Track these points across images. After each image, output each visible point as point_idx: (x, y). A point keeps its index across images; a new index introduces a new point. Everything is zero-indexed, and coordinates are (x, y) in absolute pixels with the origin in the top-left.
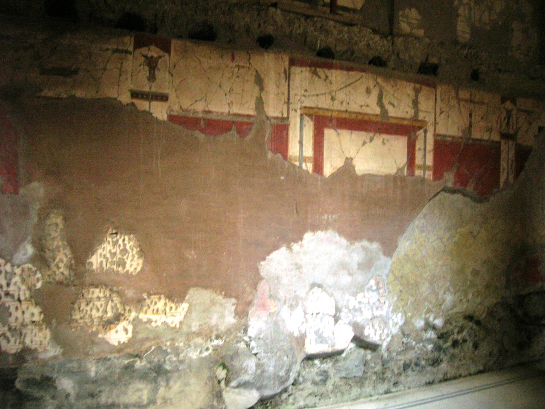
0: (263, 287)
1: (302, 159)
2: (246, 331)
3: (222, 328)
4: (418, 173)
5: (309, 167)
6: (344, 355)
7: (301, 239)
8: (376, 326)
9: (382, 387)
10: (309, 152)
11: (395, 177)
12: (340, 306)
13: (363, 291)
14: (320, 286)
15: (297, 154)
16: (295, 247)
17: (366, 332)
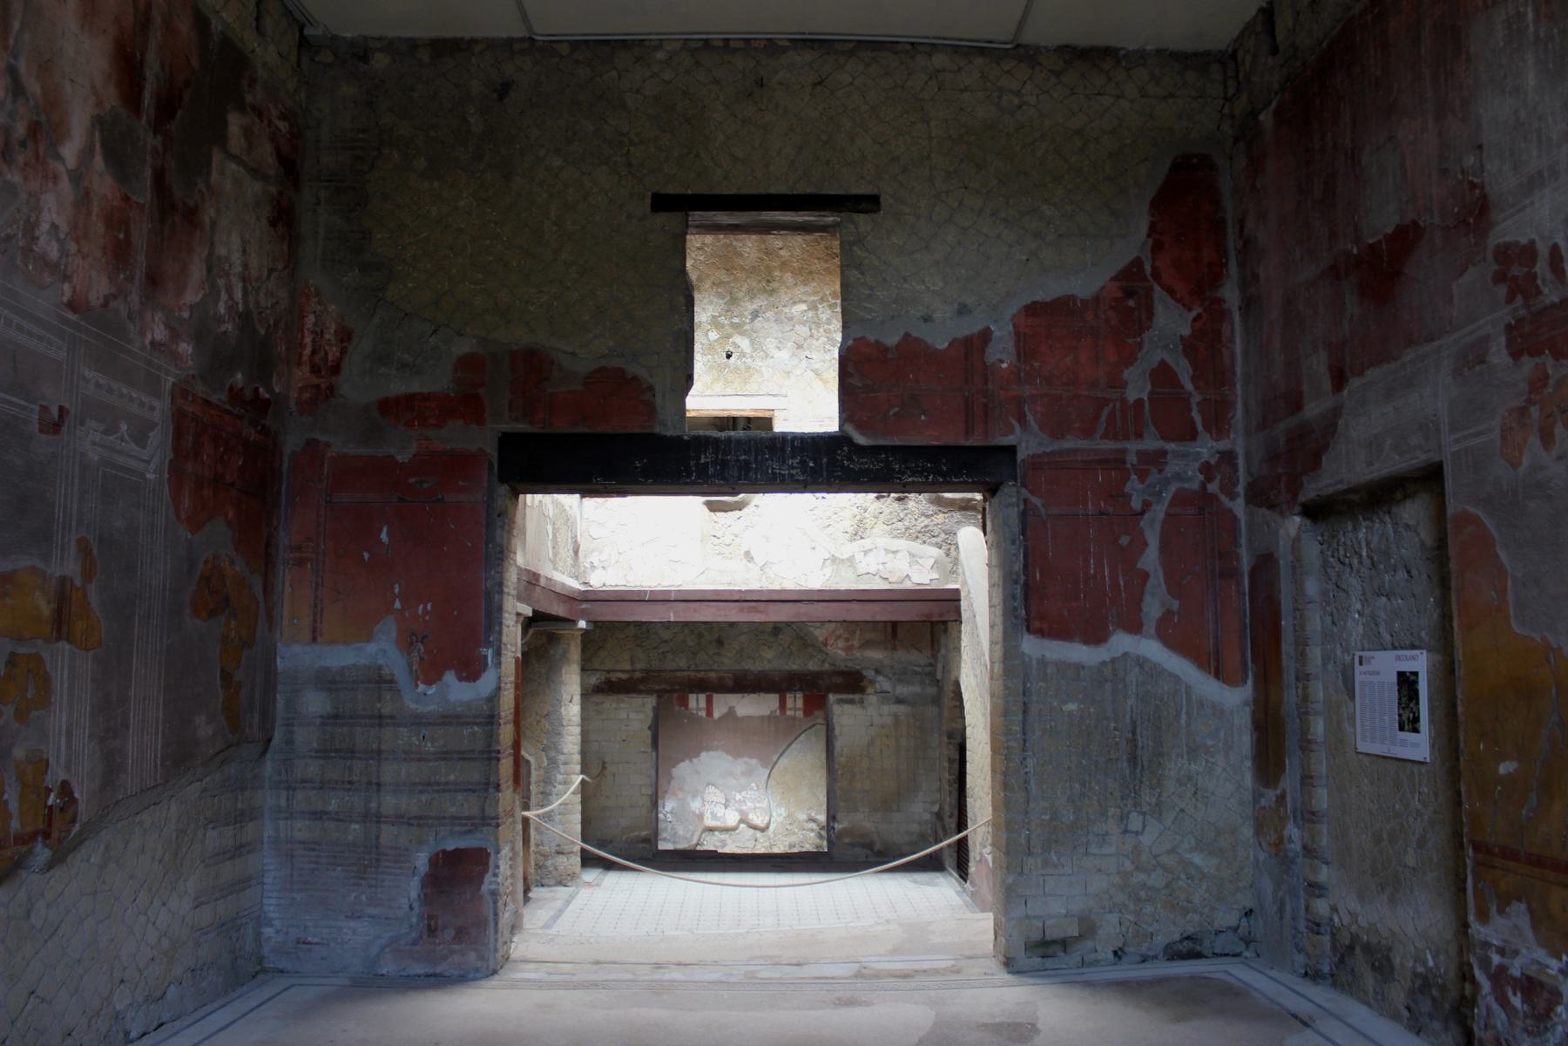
0: (673, 782)
1: (698, 709)
4: (789, 713)
5: (703, 714)
6: (737, 831)
7: (699, 756)
8: (758, 814)
10: (703, 704)
11: (769, 716)
14: (713, 785)
16: (695, 760)
17: (750, 816)
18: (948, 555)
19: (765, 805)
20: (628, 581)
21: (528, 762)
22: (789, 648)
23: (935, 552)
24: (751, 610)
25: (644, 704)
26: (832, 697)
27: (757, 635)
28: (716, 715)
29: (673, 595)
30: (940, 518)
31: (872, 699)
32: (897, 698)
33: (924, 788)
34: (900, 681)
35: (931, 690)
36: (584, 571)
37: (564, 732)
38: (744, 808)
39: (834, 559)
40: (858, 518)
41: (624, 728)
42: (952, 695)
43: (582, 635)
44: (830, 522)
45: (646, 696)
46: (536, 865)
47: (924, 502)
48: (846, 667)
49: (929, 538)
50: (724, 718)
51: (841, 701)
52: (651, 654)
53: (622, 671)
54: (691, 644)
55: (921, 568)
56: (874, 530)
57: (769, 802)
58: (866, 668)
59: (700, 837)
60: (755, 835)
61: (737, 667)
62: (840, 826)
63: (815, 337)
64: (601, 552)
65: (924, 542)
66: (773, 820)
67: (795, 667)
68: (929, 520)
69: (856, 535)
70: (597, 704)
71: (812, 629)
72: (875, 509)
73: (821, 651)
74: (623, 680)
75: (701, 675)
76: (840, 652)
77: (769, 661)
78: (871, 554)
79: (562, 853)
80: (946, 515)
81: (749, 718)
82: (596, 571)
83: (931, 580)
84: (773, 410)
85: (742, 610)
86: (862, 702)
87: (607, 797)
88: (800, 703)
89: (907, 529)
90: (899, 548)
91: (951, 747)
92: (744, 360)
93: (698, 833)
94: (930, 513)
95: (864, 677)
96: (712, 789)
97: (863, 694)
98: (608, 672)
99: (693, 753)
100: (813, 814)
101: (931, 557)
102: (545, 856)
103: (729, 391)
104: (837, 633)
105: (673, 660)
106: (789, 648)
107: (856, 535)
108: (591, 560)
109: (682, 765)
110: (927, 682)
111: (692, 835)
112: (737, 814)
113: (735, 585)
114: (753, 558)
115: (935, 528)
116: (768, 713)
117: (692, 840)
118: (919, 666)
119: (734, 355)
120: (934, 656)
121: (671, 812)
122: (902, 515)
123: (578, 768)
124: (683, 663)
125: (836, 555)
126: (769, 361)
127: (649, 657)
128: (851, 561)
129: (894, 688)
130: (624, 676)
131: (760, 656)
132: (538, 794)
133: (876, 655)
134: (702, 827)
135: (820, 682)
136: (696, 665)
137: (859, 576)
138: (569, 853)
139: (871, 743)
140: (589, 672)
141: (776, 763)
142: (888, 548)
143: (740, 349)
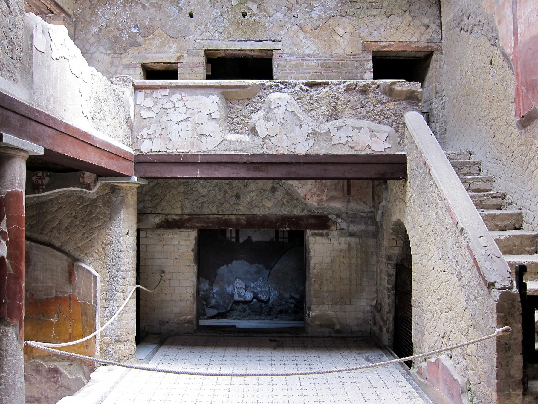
1: (231, 237)
2: (212, 290)
3: (205, 289)
4: (280, 240)
5: (234, 240)
6: (252, 303)
7: (232, 263)
9: (269, 317)
12: (247, 285)
13: (257, 281)
14: (239, 278)
15: (230, 236)
16: (230, 265)
17: (259, 295)
18: (397, 132)
19: (267, 289)
21: (95, 277)
23: (388, 129)
24: (255, 170)
25: (189, 236)
27: (261, 192)
28: (241, 241)
29: (200, 158)
30: (392, 105)
31: (335, 233)
32: (350, 233)
33: (366, 290)
34: (352, 222)
35: (372, 228)
36: (137, 142)
37: (122, 255)
38: (256, 291)
39: (315, 133)
40: (332, 105)
41: (176, 250)
42: (392, 231)
43: (138, 188)
45: (190, 230)
46: (101, 350)
47: (380, 94)
48: (318, 212)
50: (245, 242)
52: (194, 204)
53: (175, 215)
54: (220, 197)
57: (269, 288)
58: (331, 214)
59: (232, 306)
60: (261, 305)
61: (249, 213)
62: (313, 314)
63: (300, 3)
64: (149, 129)
65: (380, 122)
66: (271, 297)
67: (285, 213)
68: (384, 106)
69: (331, 116)
70: (160, 235)
71: (296, 188)
73: (302, 202)
74: (176, 220)
75: (226, 217)
76: (314, 203)
77: (269, 209)
79: (120, 342)
80: (396, 103)
81: (258, 243)
83: (385, 149)
84: (272, 50)
85: (249, 170)
86: (328, 235)
87: (166, 294)
90: (362, 126)
91: (390, 266)
93: (230, 305)
94: (384, 101)
95: (330, 219)
96: (238, 281)
97: (329, 230)
98: (167, 215)
99: (228, 262)
100: (293, 295)
102: (108, 344)
104: (312, 191)
105: (208, 207)
107: (331, 116)
108: (142, 133)
109: (222, 268)
110: (369, 223)
111: (228, 305)
112: (252, 294)
113: (244, 152)
114: (257, 133)
115: (388, 112)
116: (269, 240)
117: (227, 308)
118: (365, 212)
120: (375, 206)
121: (216, 293)
122: (364, 103)
123: (134, 280)
124: (214, 210)
125: (317, 130)
126: (270, 19)
127: (193, 205)
129: (349, 226)
130: (176, 218)
131: (263, 205)
132: (103, 299)
133: (337, 205)
134: (234, 301)
135: (302, 222)
136: (222, 211)
137: (333, 145)
138: (125, 341)
139: (333, 262)
140: (155, 215)
142: (355, 125)
143: (251, 11)
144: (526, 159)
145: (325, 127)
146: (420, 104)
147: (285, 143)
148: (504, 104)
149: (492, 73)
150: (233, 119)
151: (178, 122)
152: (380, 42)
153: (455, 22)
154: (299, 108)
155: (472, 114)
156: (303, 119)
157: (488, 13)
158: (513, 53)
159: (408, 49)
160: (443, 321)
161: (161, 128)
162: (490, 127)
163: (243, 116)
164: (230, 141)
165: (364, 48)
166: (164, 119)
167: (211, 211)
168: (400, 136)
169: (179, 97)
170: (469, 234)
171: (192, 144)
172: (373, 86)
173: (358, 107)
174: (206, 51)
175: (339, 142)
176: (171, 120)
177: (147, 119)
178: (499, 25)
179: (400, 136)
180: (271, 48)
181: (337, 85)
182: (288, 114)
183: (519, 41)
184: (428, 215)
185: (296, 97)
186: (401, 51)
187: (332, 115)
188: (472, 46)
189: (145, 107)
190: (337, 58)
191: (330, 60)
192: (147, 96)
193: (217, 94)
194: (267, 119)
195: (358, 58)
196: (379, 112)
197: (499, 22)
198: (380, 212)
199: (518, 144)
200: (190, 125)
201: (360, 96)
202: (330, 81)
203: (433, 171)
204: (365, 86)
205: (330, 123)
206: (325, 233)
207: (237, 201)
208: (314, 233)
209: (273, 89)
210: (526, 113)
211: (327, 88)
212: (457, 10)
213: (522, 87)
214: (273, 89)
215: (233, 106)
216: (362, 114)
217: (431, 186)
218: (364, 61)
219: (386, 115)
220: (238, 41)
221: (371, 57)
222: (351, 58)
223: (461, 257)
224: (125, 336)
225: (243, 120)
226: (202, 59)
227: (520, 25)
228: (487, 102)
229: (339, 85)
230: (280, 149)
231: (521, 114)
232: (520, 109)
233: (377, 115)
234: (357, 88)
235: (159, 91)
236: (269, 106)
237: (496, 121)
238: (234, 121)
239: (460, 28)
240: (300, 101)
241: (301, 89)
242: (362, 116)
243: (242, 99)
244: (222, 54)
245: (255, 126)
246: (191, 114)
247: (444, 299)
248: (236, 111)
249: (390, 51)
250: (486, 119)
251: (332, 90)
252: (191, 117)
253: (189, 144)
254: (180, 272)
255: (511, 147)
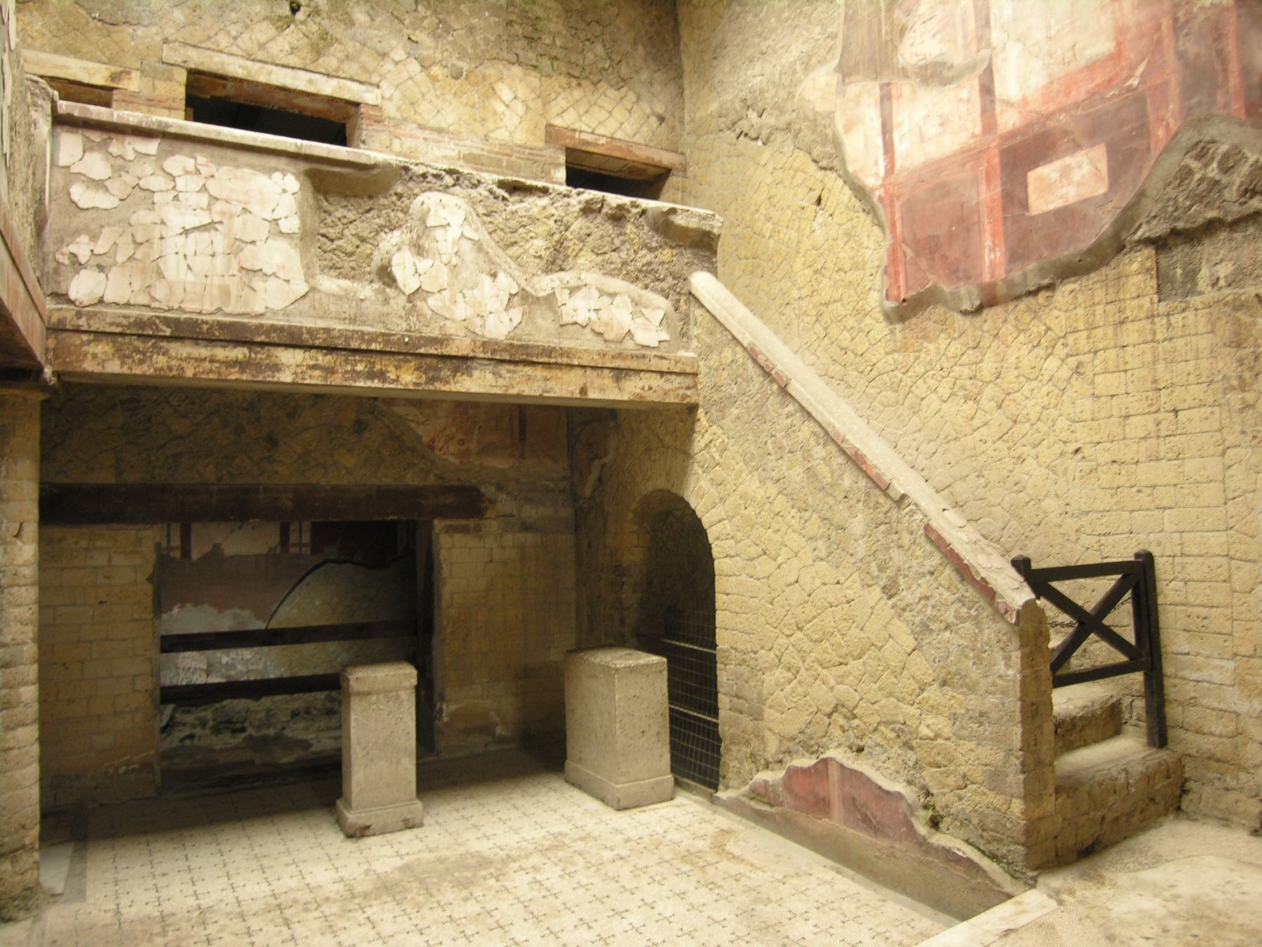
4: (292, 550)
5: (177, 554)
20: (154, 299)
22: (378, 451)
25: (139, 541)
26: (438, 524)
28: (195, 555)
30: (666, 254)
31: (493, 525)
36: (56, 272)
40: (557, 237)
44: (515, 237)
45: (141, 526)
47: (646, 228)
49: (653, 281)
50: (206, 558)
51: (451, 530)
52: (153, 458)
55: (647, 322)
56: (581, 261)
64: (94, 238)
65: (646, 287)
72: (581, 228)
73: (423, 457)
76: (452, 459)
78: (579, 294)
80: (675, 251)
82: (83, 272)
84: (357, 105)
86: (478, 529)
88: (306, 538)
89: (624, 263)
90: (617, 291)
92: (318, 19)
94: (654, 244)
95: (483, 495)
101: (661, 308)
103: (293, 60)
104: (448, 432)
106: (378, 451)
107: (553, 263)
108: (72, 248)
113: (364, 323)
115: (660, 267)
119: (302, 9)
122: (617, 242)
125: (528, 288)
128: (550, 300)
133: (499, 463)
137: (562, 326)
141: (275, 612)
144: (904, 377)
145: (545, 284)
146: (714, 260)
147: (461, 311)
148: (851, 276)
149: (820, 219)
150: (332, 241)
151: (186, 232)
152: (581, 131)
153: (724, 119)
154: (487, 236)
155: (767, 293)
156: (498, 260)
157: (817, 110)
158: (882, 186)
159: (628, 158)
160: (832, 682)
161: (135, 242)
162: (814, 319)
163: (356, 235)
164: (327, 294)
165: (550, 138)
166: (143, 216)
167: (200, 475)
168: (681, 320)
169: (190, 163)
170: (923, 505)
171: (225, 292)
172: (634, 211)
173: (607, 249)
174: (192, 72)
175: (574, 320)
176: (163, 223)
177: (90, 212)
178: (846, 133)
179: (681, 320)
180: (355, 99)
181: (565, 196)
182: (466, 247)
183: (898, 166)
184: (775, 475)
185: (481, 210)
186: (617, 158)
187: (556, 261)
188: (770, 167)
189: (83, 178)
190: (497, 149)
191: (483, 149)
192: (91, 149)
193: (294, 174)
194: (419, 250)
195: (538, 155)
196: (644, 265)
197: (849, 128)
198: (592, 479)
199: (887, 350)
200: (220, 241)
201: (609, 227)
202: (550, 186)
203: (795, 388)
204: (620, 207)
205: (554, 276)
206: (472, 526)
207: (269, 450)
208: (451, 526)
209: (428, 182)
210: (914, 293)
211: (545, 201)
212: (729, 97)
213: (905, 247)
214: (428, 182)
215: (331, 208)
216: (613, 266)
217: (788, 417)
218: (550, 164)
219: (656, 272)
220: (277, 65)
221: (562, 159)
222: (524, 153)
223: (895, 553)
224: (16, 837)
225: (358, 247)
226: (181, 92)
227: (902, 138)
228: (809, 272)
229: (569, 197)
230: (447, 322)
231: (899, 296)
232: (899, 287)
233: (640, 271)
234: (605, 210)
235: (129, 139)
236: (423, 220)
237: (831, 308)
238: (334, 246)
239: (738, 131)
240: (489, 219)
241: (491, 192)
242: (613, 270)
243: (356, 196)
244: (230, 90)
245: (390, 262)
246: (223, 213)
247: (838, 638)
248: (339, 223)
249: (593, 153)
250: (804, 303)
251: (556, 205)
252: (221, 222)
253: (216, 292)
254: (112, 640)
255: (867, 356)
